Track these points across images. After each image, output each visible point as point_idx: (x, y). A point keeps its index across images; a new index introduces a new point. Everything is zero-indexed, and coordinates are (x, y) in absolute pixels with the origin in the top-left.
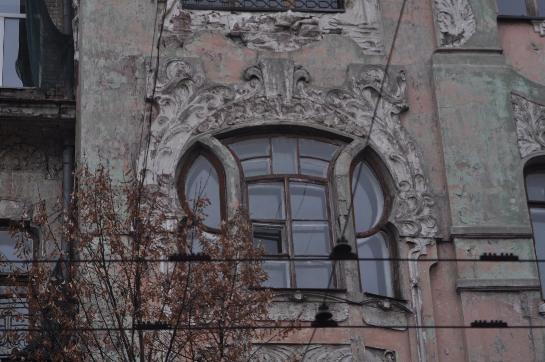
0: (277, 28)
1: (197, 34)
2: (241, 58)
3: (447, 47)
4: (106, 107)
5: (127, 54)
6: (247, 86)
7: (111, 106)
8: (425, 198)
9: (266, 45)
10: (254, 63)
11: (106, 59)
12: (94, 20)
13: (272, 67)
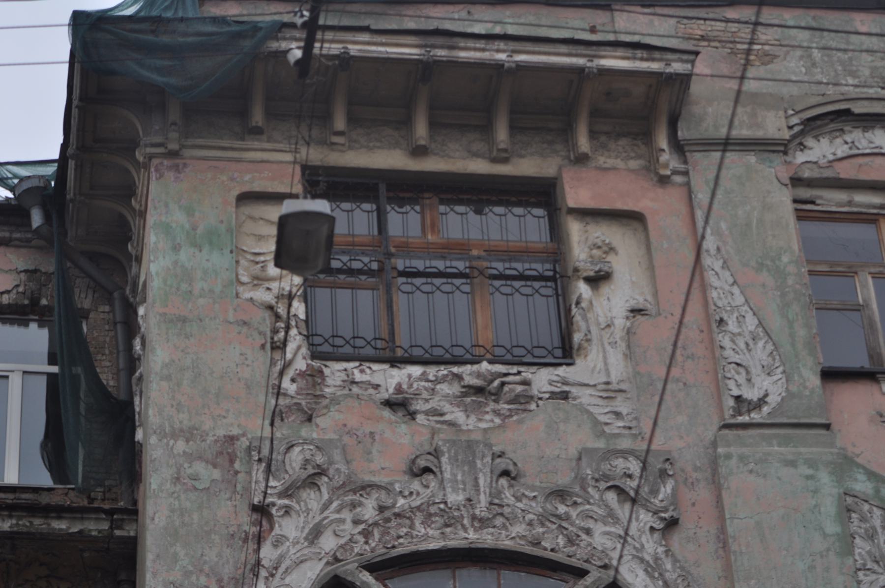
0: (464, 390)
1: (335, 400)
2: (405, 440)
3: (740, 419)
4: (186, 519)
5: (221, 432)
6: (416, 485)
7: (195, 517)
9: (447, 418)
10: (427, 448)
11: (187, 441)
12: (168, 378)
13: (456, 454)
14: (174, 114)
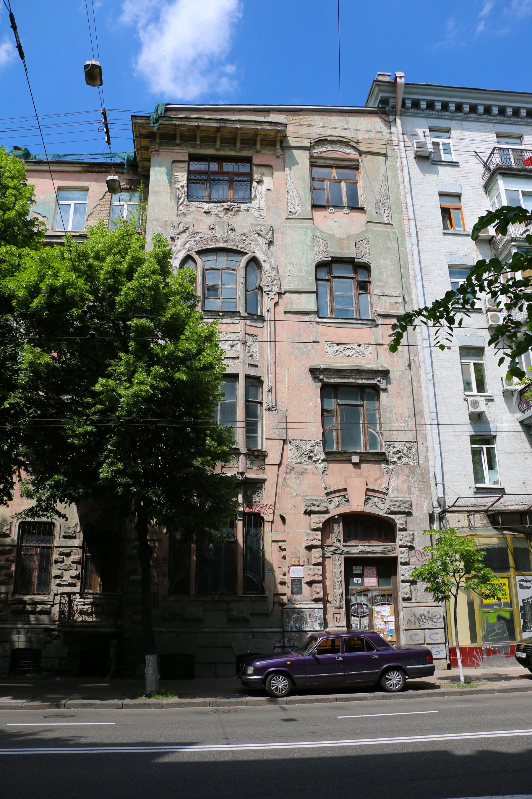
3: (290, 217)
5: (164, 219)
12: (153, 206)
14: (158, 140)
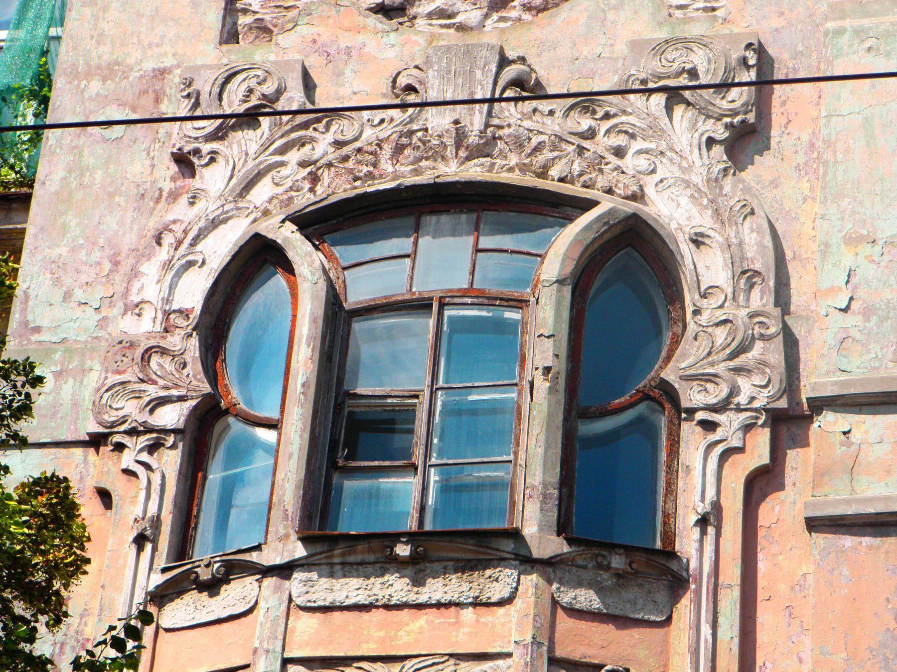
4: (87, 179)
5: (149, 65)
7: (99, 175)
8: (757, 320)
9: (458, 19)
11: (104, 80)
13: (449, 64)
